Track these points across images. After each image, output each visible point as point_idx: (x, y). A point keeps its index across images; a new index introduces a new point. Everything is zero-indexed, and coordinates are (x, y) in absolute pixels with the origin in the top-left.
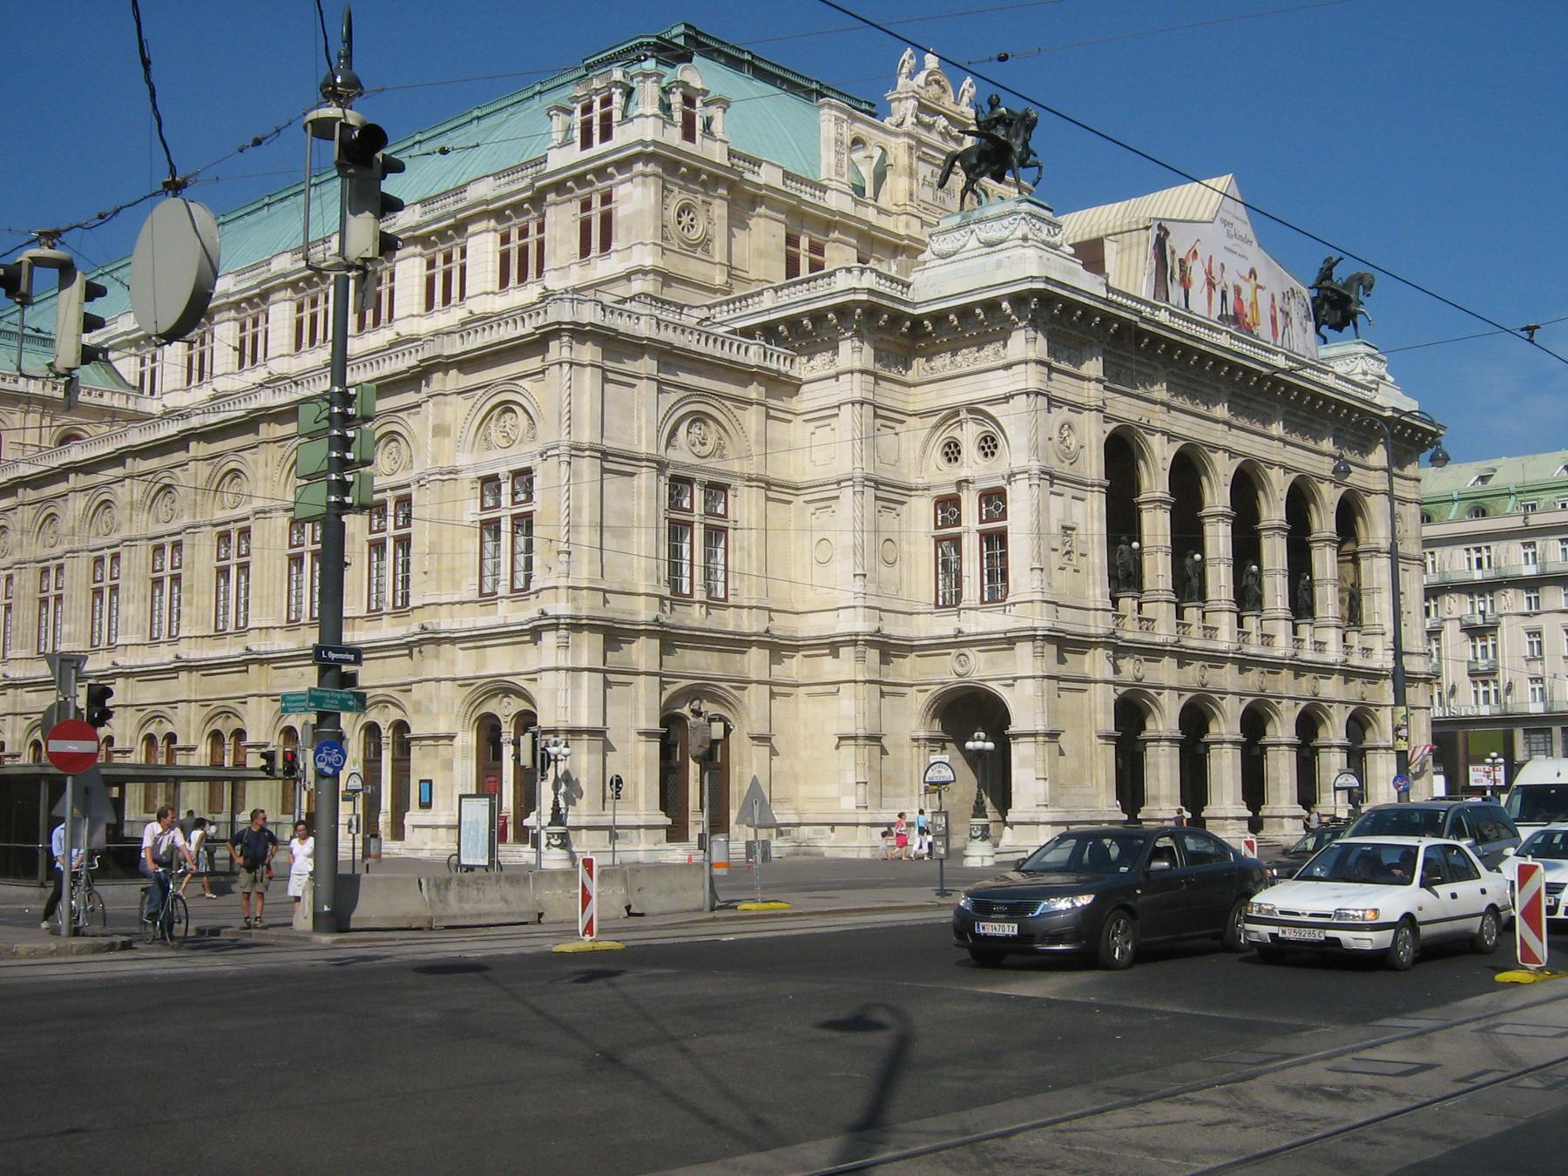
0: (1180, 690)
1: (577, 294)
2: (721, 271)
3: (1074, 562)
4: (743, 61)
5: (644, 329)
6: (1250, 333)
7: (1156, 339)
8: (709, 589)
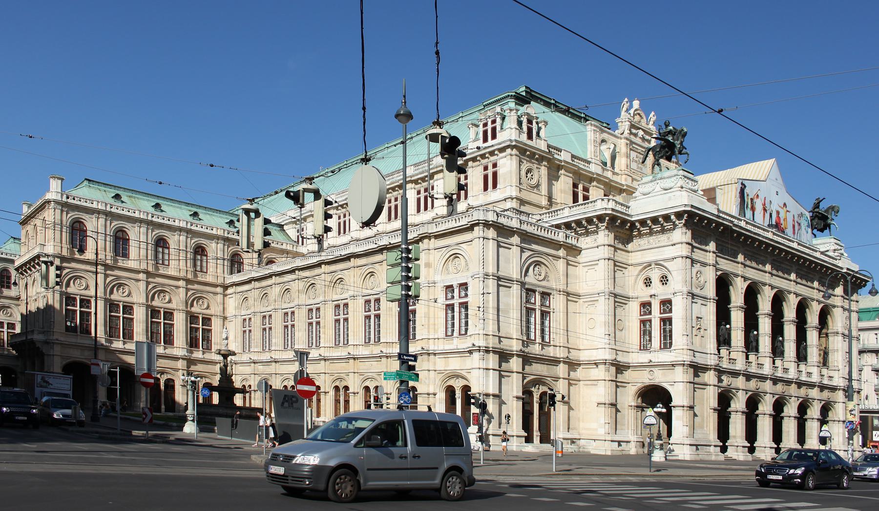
0: (746, 391)
1: (485, 207)
2: (545, 199)
3: (702, 333)
4: (551, 104)
5: (514, 224)
6: (783, 232)
7: (740, 234)
8: (543, 338)
